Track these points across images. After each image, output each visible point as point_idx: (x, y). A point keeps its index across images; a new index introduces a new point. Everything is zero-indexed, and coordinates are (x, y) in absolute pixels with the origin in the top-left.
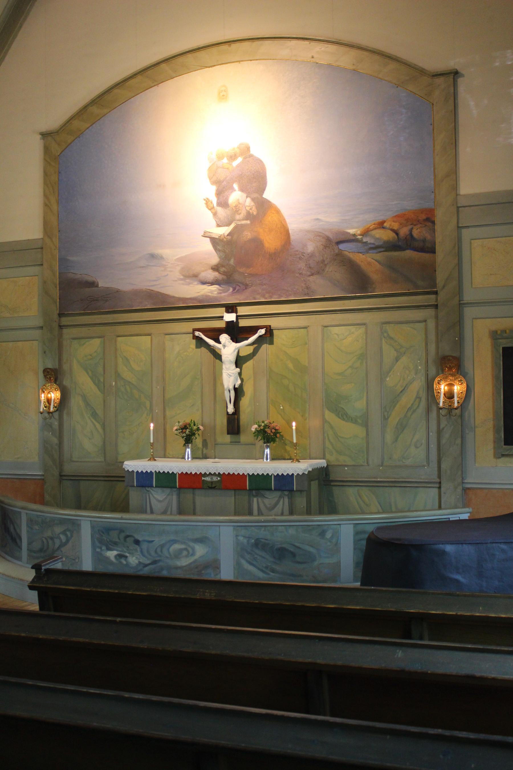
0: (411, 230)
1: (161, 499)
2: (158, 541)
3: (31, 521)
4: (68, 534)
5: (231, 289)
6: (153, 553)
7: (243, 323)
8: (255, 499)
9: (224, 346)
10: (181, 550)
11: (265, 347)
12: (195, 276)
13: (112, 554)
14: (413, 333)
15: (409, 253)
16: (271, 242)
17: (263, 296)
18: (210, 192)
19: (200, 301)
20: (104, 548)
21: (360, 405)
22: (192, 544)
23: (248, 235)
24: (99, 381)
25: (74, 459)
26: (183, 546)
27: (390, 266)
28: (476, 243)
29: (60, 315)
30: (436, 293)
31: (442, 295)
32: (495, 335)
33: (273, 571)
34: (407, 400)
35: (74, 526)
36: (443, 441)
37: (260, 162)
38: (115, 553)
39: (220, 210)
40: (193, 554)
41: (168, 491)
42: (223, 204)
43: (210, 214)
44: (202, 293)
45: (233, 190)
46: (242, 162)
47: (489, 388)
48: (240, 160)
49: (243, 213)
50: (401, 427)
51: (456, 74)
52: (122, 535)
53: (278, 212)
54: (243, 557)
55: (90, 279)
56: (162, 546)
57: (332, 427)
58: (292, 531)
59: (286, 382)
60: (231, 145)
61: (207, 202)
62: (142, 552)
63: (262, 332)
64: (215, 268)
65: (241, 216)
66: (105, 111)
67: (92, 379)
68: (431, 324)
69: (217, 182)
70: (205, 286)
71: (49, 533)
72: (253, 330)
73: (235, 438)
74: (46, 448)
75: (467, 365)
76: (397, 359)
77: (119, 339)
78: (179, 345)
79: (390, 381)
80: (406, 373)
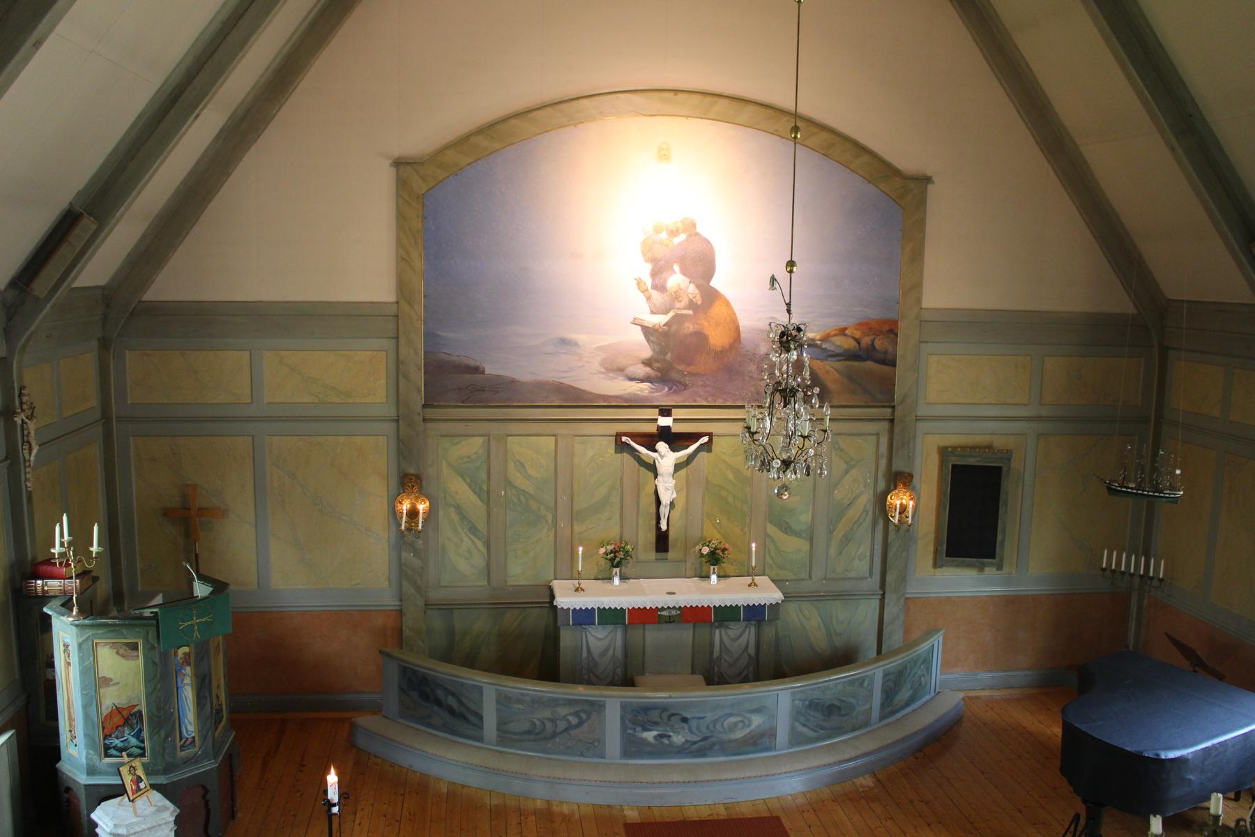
0: (873, 341)
1: (601, 636)
2: (710, 716)
3: (508, 698)
4: (584, 716)
5: (667, 389)
6: (704, 729)
7: (678, 428)
8: (717, 631)
9: (662, 457)
10: (736, 724)
11: (702, 454)
12: (621, 370)
13: (650, 735)
14: (867, 444)
15: (869, 365)
16: (718, 338)
17: (706, 400)
18: (645, 271)
19: (627, 400)
20: (639, 729)
21: (806, 518)
22: (748, 715)
23: (689, 327)
24: (481, 489)
25: (443, 583)
26: (739, 719)
27: (851, 377)
28: (933, 359)
29: (424, 406)
30: (893, 407)
31: (898, 412)
32: (944, 452)
33: (822, 728)
34: (852, 514)
35: (596, 707)
36: (890, 555)
37: (708, 242)
38: (655, 733)
39: (654, 293)
40: (749, 725)
41: (610, 627)
42: (660, 288)
43: (642, 297)
44: (630, 390)
45: (674, 272)
46: (687, 240)
47: (933, 504)
48: (682, 237)
49: (685, 302)
50: (847, 540)
51: (926, 180)
52: (665, 715)
53: (728, 304)
54: (797, 720)
55: (472, 363)
56: (715, 722)
57: (773, 541)
58: (840, 687)
59: (724, 493)
60: (672, 218)
61: (639, 283)
62: (690, 729)
63: (706, 439)
64: (647, 363)
65: (682, 304)
66: (497, 145)
67: (470, 485)
68: (884, 440)
69: (653, 260)
70: (633, 383)
71: (547, 714)
72: (694, 437)
73: (663, 555)
74: (402, 572)
75: (916, 481)
76: (847, 472)
77: (510, 438)
78: (594, 449)
79: (838, 494)
80: (857, 489)
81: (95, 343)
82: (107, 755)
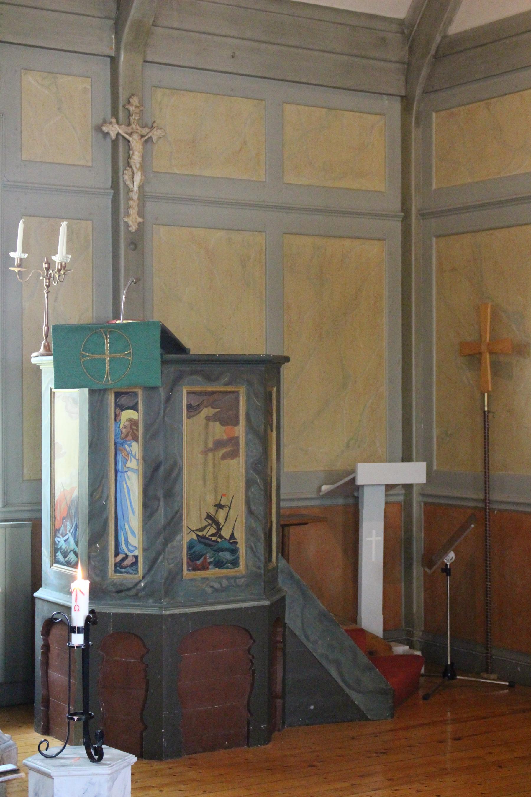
81: (397, 106)
82: (57, 561)
